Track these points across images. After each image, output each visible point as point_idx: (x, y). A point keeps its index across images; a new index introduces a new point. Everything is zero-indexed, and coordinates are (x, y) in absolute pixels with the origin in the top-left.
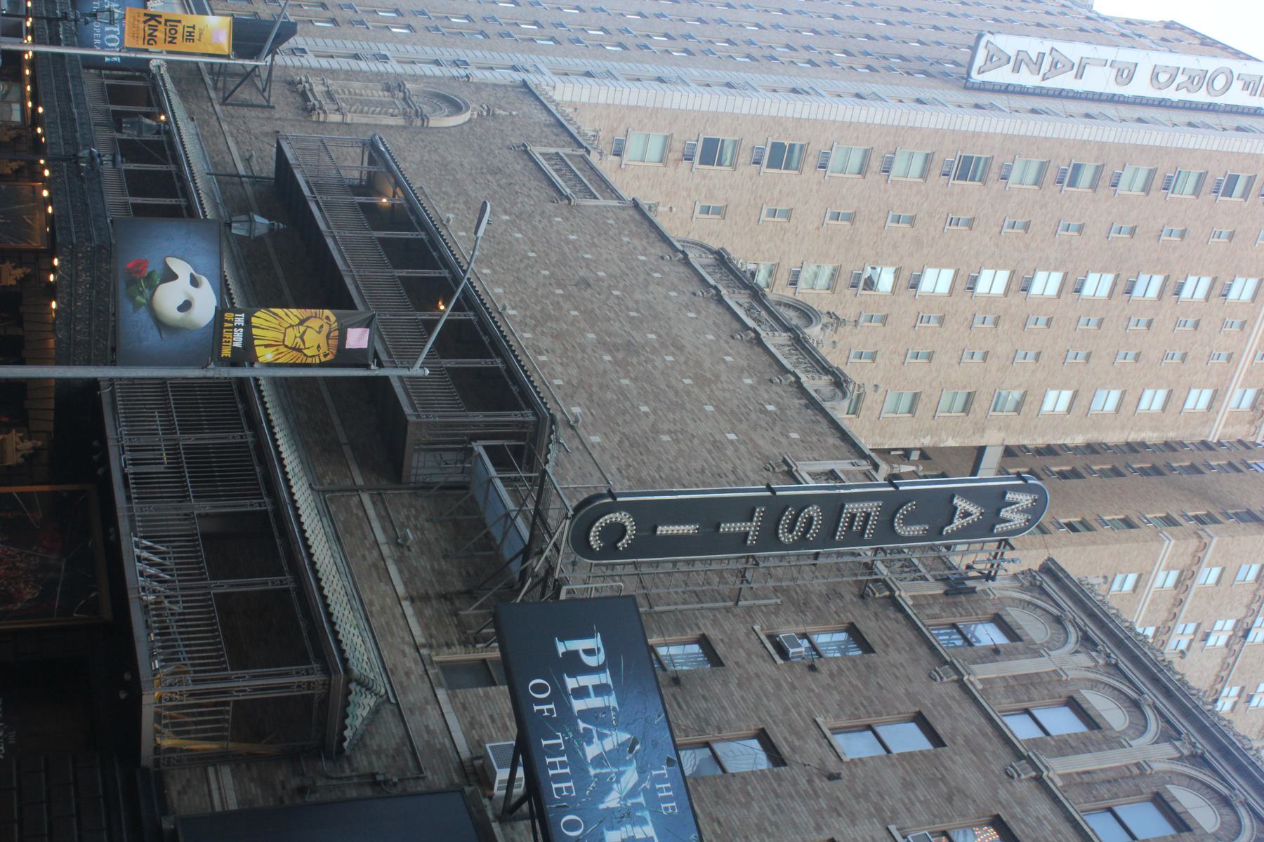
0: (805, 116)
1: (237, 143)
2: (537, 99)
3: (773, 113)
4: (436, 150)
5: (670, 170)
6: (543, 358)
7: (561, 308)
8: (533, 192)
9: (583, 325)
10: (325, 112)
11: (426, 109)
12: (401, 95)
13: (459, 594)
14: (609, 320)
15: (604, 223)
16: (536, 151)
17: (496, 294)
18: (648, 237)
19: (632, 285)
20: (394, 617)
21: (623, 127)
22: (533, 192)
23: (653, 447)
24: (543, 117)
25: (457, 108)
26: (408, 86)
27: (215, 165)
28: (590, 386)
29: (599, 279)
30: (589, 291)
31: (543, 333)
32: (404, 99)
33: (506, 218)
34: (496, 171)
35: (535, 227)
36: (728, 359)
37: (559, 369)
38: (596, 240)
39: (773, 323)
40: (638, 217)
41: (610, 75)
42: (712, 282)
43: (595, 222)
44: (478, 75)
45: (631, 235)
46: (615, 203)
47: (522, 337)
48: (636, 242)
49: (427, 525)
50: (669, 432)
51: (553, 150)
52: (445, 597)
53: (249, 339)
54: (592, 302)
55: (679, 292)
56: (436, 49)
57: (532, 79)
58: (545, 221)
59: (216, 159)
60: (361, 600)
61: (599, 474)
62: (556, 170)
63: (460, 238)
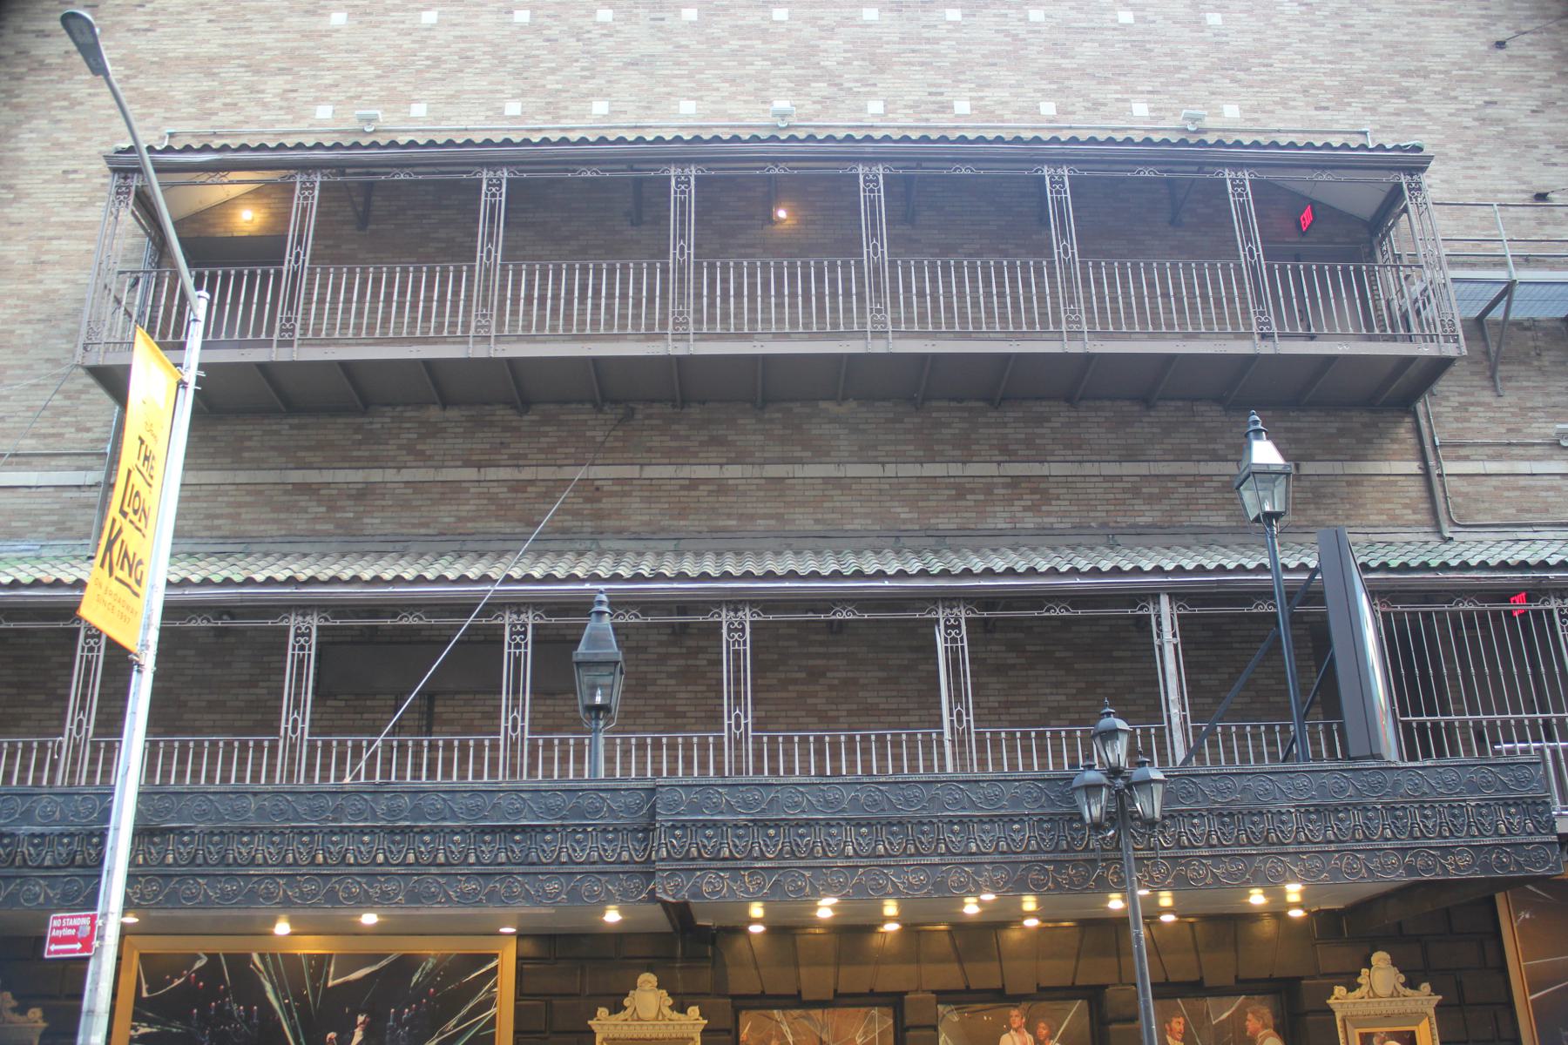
6: (962, 107)
28: (1059, 68)
49: (1509, 398)
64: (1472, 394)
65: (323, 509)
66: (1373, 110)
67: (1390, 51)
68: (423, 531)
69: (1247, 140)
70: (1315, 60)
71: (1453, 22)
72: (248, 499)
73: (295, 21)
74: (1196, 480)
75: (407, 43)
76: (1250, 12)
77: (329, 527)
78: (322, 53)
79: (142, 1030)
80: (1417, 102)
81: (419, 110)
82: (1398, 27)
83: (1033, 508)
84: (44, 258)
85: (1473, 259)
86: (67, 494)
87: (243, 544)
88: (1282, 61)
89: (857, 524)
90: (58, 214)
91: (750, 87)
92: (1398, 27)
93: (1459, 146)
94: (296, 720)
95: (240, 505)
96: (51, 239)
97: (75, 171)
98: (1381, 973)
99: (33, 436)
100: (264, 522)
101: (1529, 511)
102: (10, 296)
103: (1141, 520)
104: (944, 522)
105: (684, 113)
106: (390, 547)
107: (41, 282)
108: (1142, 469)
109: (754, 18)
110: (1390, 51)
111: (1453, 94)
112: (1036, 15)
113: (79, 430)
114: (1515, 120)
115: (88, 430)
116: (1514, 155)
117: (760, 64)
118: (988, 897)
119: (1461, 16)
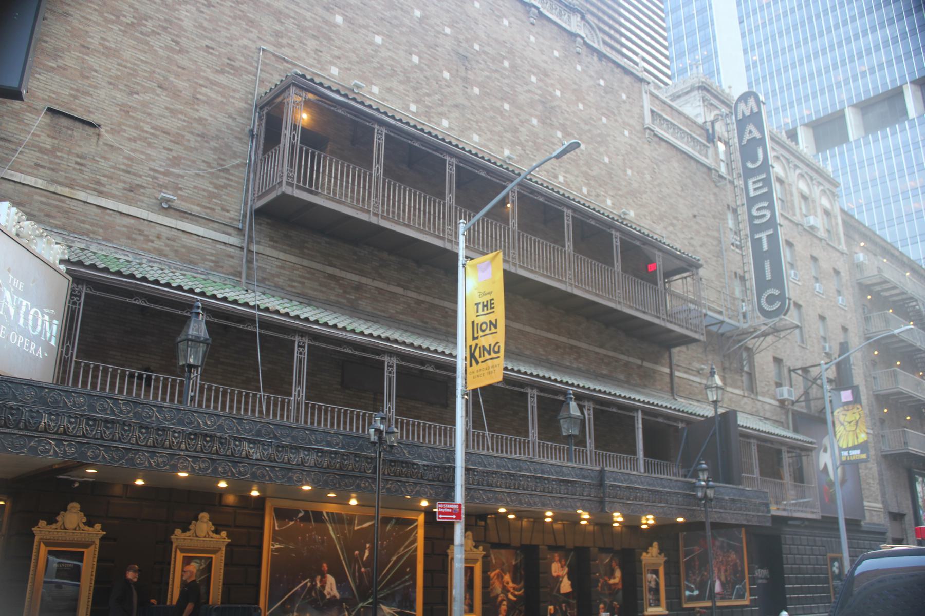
6: (561, 179)
52: (724, 369)
53: (854, 448)
65: (341, 291)
68: (383, 314)
72: (307, 275)
73: (320, 10)
74: (617, 360)
77: (344, 301)
78: (333, 36)
79: (277, 546)
84: (198, 96)
86: (219, 246)
87: (307, 300)
89: (527, 352)
90: (204, 71)
94: (299, 391)
95: (304, 278)
96: (201, 85)
97: (213, 49)
98: (654, 549)
99: (199, 205)
100: (316, 290)
102: (182, 113)
103: (604, 372)
104: (553, 359)
105: (474, 141)
106: (371, 318)
107: (198, 111)
109: (498, 104)
113: (224, 210)
115: (228, 211)
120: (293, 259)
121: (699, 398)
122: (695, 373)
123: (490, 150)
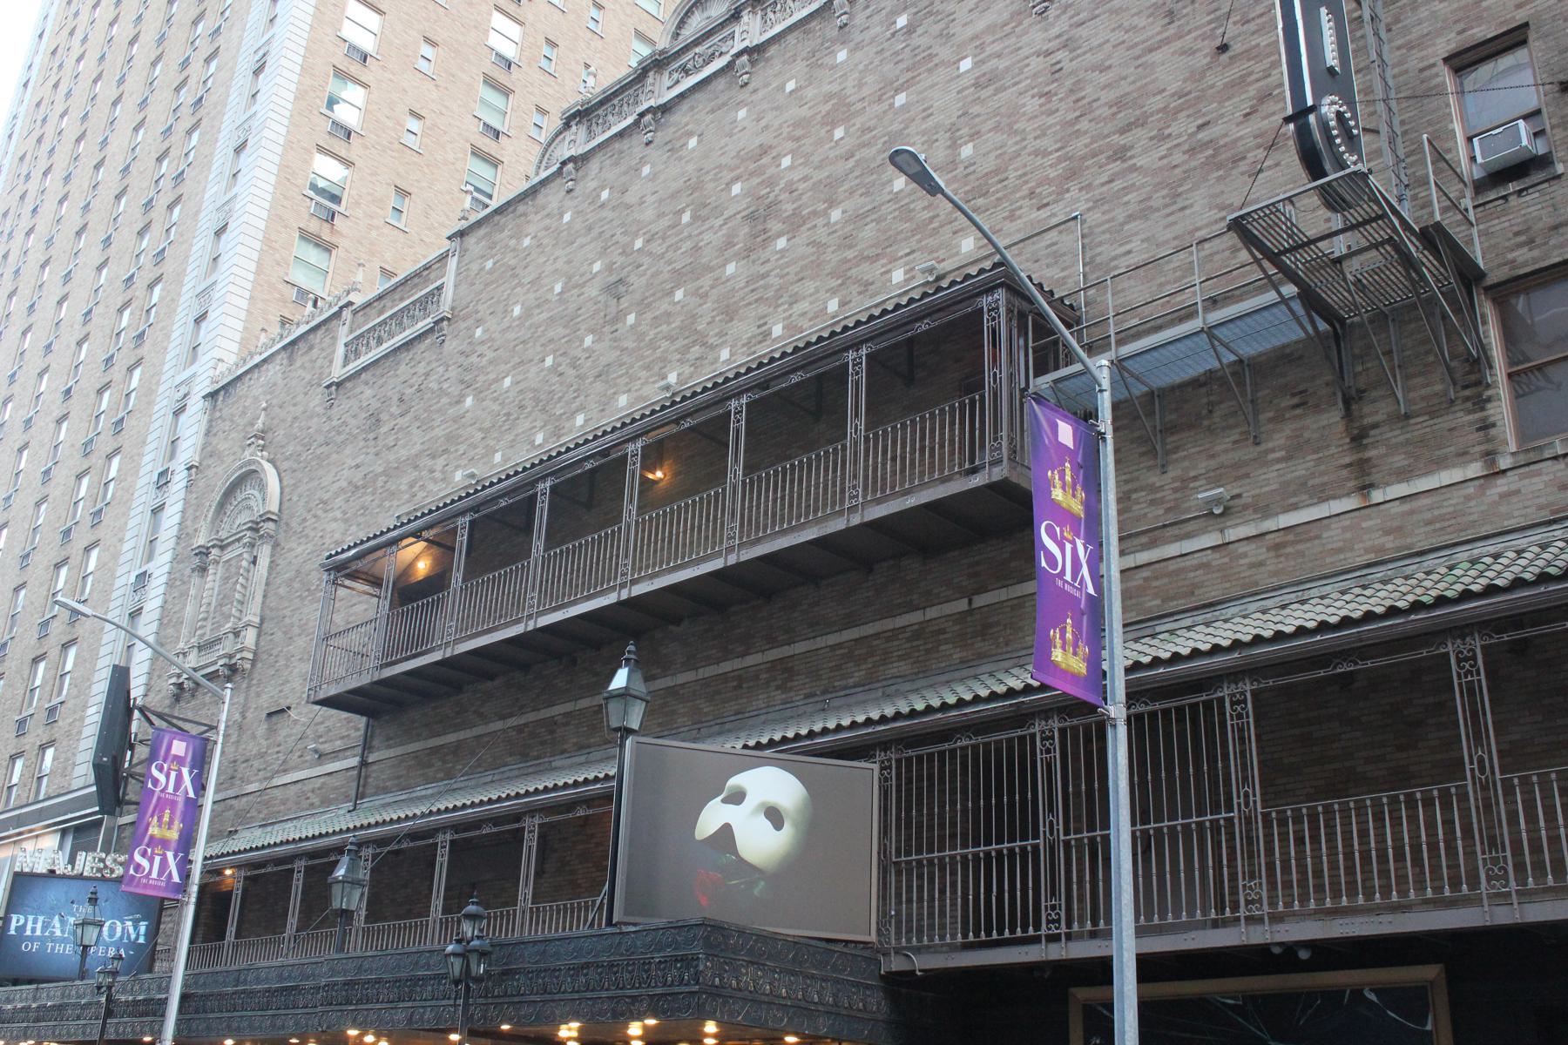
0: (299, 60)
1: (285, 771)
2: (239, 378)
3: (291, 97)
4: (325, 503)
5: (342, 243)
6: (777, 330)
7: (668, 314)
8: (421, 369)
9: (706, 282)
10: (241, 650)
11: (244, 518)
12: (214, 551)
13: (1348, 414)
14: (696, 248)
15: (491, 272)
16: (338, 372)
17: (631, 405)
18: (525, 214)
19: (622, 225)
20: (1412, 512)
21: (283, 287)
22: (421, 369)
23: (990, 164)
24: (273, 370)
25: (248, 477)
26: (201, 540)
27: (326, 802)
28: (846, 261)
29: (609, 268)
30: (632, 279)
31: (721, 334)
32: (222, 548)
33: (469, 401)
34: (375, 420)
35: (490, 363)
36: (790, 86)
37: (803, 306)
38: (526, 281)
39: (716, 39)
40: (482, 231)
41: (205, 294)
42: (630, 120)
43: (487, 285)
44: (188, 451)
45: (519, 236)
46: (452, 263)
47: (728, 362)
48: (532, 229)
49: (1174, 472)
50: (954, 145)
51: (340, 351)
52: (1358, 439)
54: (658, 273)
55: (642, 161)
56: (132, 513)
57: (203, 386)
58: (480, 349)
59: (316, 801)
60: (1369, 566)
61: (1053, 234)
62: (380, 341)
63: (505, 460)
64: (1137, 479)
66: (1089, 187)
67: (1114, 109)
69: (973, 271)
70: (1046, 153)
71: (1177, 45)
74: (895, 633)
75: (496, 407)
76: (996, 128)
80: (1131, 157)
81: (498, 457)
82: (1125, 78)
83: (782, 687)
85: (1159, 321)
88: (1016, 170)
91: (656, 369)
92: (1125, 78)
93: (1165, 192)
101: (1173, 599)
103: (851, 681)
105: (624, 404)
108: (854, 633)
110: (1114, 109)
111: (1166, 132)
112: (836, 215)
114: (1226, 135)
116: (1219, 179)
117: (665, 344)
118: (651, 1022)
119: (1190, 32)
120: (399, 751)
121: (1214, 594)
122: (1201, 523)
123: (644, 399)
